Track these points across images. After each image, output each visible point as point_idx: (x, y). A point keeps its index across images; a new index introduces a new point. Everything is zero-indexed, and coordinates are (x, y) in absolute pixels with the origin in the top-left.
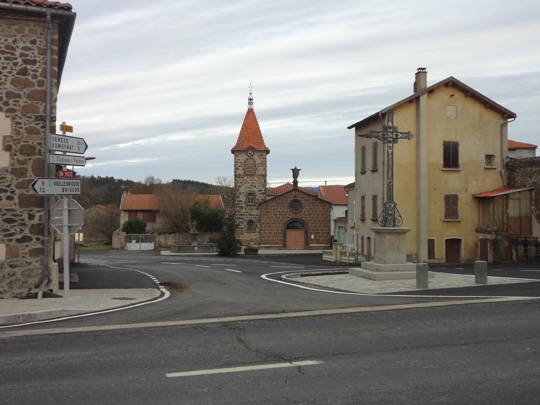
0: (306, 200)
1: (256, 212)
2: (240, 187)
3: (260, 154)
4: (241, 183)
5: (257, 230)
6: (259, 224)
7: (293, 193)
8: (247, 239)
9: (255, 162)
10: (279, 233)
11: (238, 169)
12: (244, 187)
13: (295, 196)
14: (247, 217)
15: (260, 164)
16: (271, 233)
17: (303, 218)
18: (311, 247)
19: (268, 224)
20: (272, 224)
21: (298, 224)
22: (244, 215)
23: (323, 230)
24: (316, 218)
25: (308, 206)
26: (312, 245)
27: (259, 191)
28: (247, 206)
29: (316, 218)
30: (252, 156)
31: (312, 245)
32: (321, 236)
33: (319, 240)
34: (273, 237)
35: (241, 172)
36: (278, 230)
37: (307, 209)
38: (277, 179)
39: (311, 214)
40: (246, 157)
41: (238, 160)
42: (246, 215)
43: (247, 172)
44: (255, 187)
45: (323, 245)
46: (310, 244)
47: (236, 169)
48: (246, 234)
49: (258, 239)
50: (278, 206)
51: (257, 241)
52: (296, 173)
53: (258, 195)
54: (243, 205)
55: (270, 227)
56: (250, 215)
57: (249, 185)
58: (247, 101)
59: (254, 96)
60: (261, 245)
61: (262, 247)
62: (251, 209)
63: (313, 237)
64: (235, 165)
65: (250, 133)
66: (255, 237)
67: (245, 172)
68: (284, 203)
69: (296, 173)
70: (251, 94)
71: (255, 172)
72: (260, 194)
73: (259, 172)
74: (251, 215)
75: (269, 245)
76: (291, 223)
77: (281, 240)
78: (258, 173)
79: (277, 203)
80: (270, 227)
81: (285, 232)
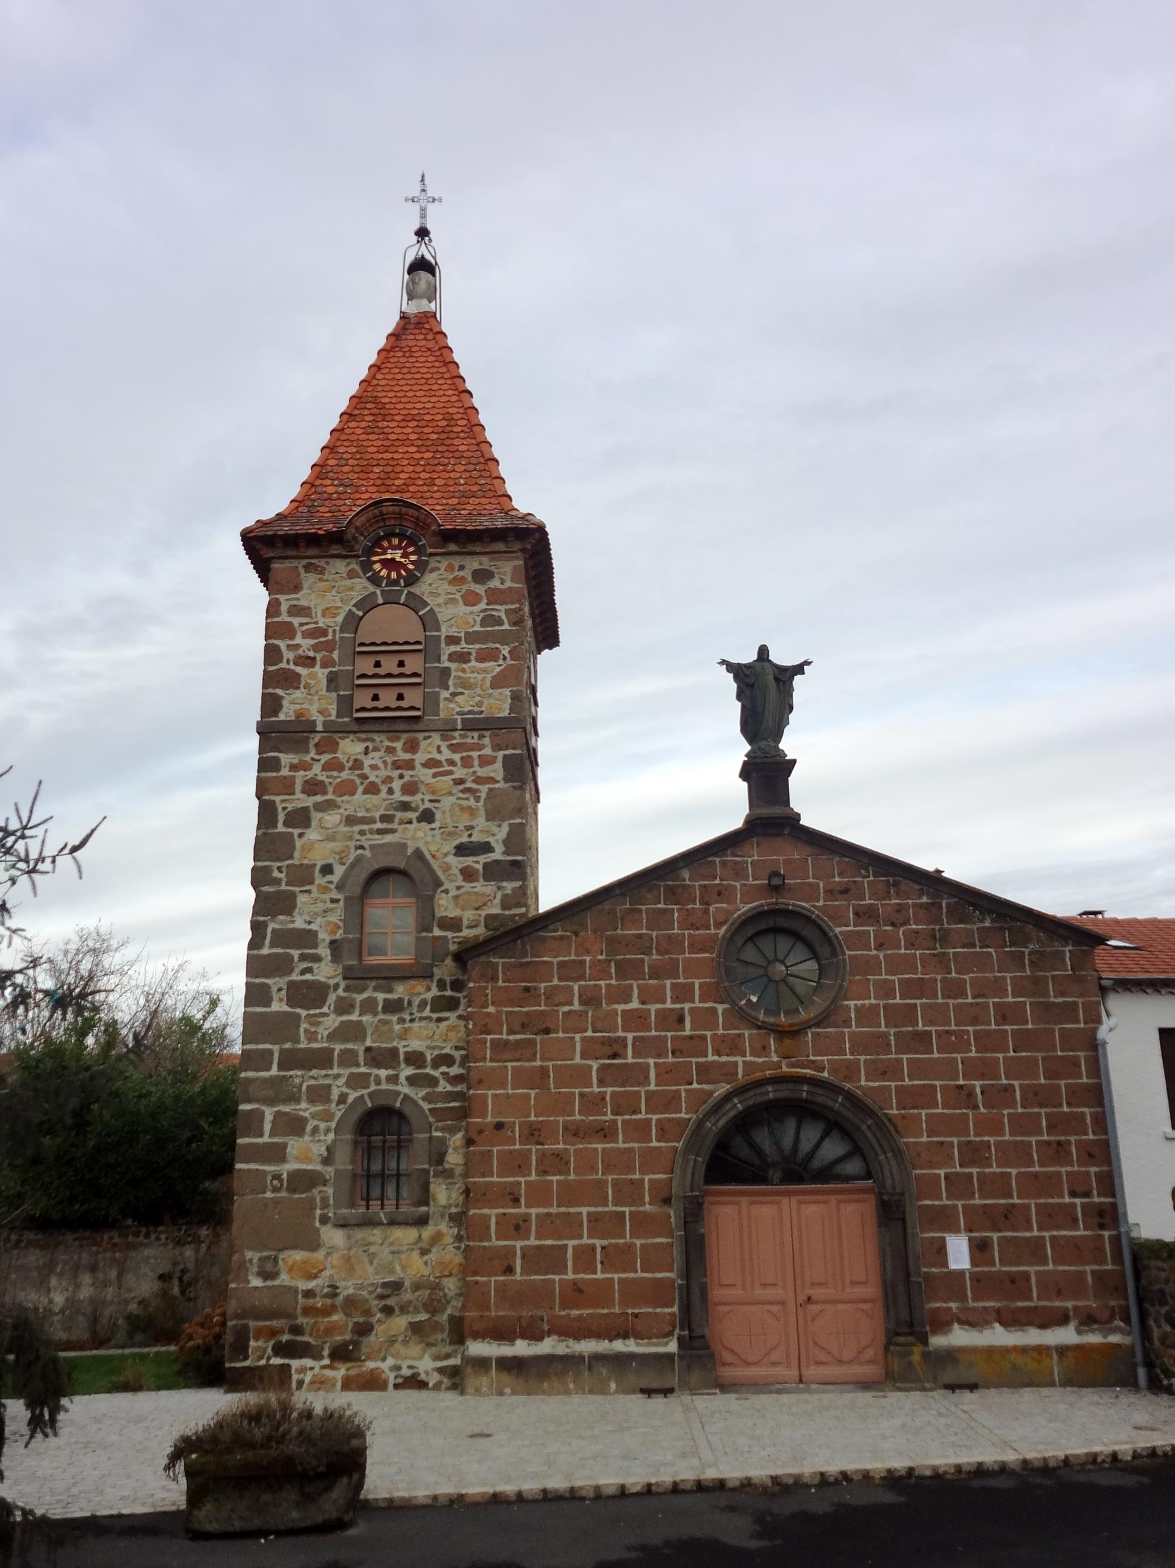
0: (865, 915)
1: (426, 1035)
2: (300, 818)
3: (473, 564)
4: (313, 787)
5: (443, 1194)
6: (457, 1139)
7: (752, 855)
8: (348, 1288)
9: (429, 621)
10: (641, 1224)
11: (289, 680)
12: (332, 819)
13: (776, 884)
14: (356, 1081)
15: (471, 638)
16: (571, 1225)
17: (851, 1070)
18: (950, 1356)
19: (533, 1133)
20: (575, 1132)
21: (810, 1134)
22: (322, 1059)
23: (1047, 1184)
24: (975, 1069)
25: (895, 965)
26: (960, 1337)
27: (462, 850)
28: (357, 977)
29: (975, 1069)
30: (412, 580)
31: (960, 1337)
32: (1035, 1251)
33: (1017, 1284)
34: (585, 1258)
35: (313, 701)
36: (629, 1192)
37: (886, 990)
38: (621, 789)
39: (922, 1039)
40: (361, 587)
41: (296, 611)
42: (348, 1059)
43: (362, 699)
44: (427, 817)
45: (1066, 1335)
46: (941, 1324)
47: (277, 678)
48: (333, 1237)
49: (451, 1285)
50: (622, 973)
51: (434, 1307)
52: (764, 693)
53: (453, 883)
54: (325, 971)
55: (558, 1162)
56: (378, 1058)
57: (377, 804)
58: (397, 277)
59: (440, 249)
60: (477, 1348)
61: (482, 1363)
62: (393, 1007)
63: (958, 1253)
64: (271, 654)
65: (405, 441)
66: (416, 1267)
67: (345, 704)
68: (673, 944)
69: (764, 693)
70: (422, 233)
71: (431, 701)
72: (468, 874)
73: (466, 702)
74: (383, 1058)
75: (548, 1346)
76: (744, 1124)
77: (657, 1293)
78: (454, 705)
79: (614, 944)
80: (558, 1162)
81: (694, 1213)
